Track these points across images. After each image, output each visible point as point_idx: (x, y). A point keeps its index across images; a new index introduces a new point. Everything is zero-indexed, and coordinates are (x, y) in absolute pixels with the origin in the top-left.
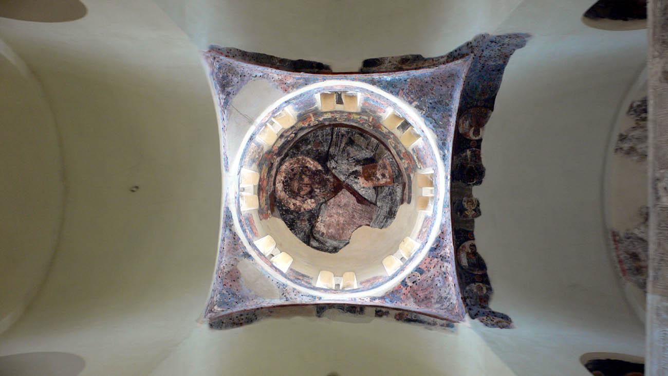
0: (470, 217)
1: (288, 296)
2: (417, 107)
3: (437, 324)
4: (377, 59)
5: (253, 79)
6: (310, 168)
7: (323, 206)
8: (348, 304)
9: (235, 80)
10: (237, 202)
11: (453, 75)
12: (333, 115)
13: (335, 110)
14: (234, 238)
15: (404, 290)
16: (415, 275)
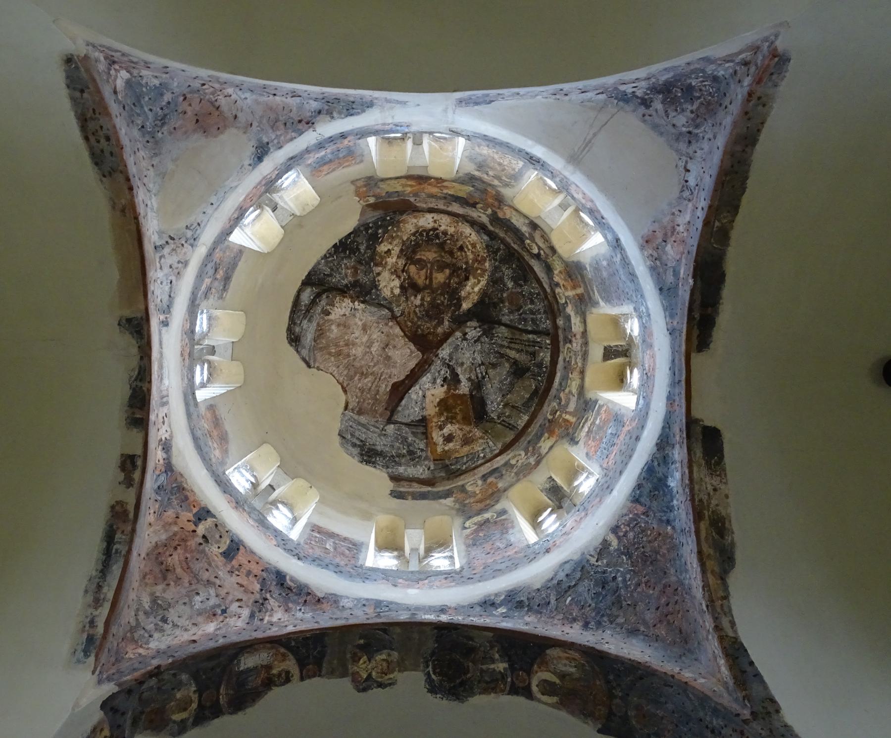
0: (352, 668)
2: (605, 544)
3: (96, 609)
7: (385, 312)
10: (387, 128)
11: (686, 643)
12: (578, 336)
13: (590, 340)
14: (300, 121)
15: (187, 515)
16: (223, 540)
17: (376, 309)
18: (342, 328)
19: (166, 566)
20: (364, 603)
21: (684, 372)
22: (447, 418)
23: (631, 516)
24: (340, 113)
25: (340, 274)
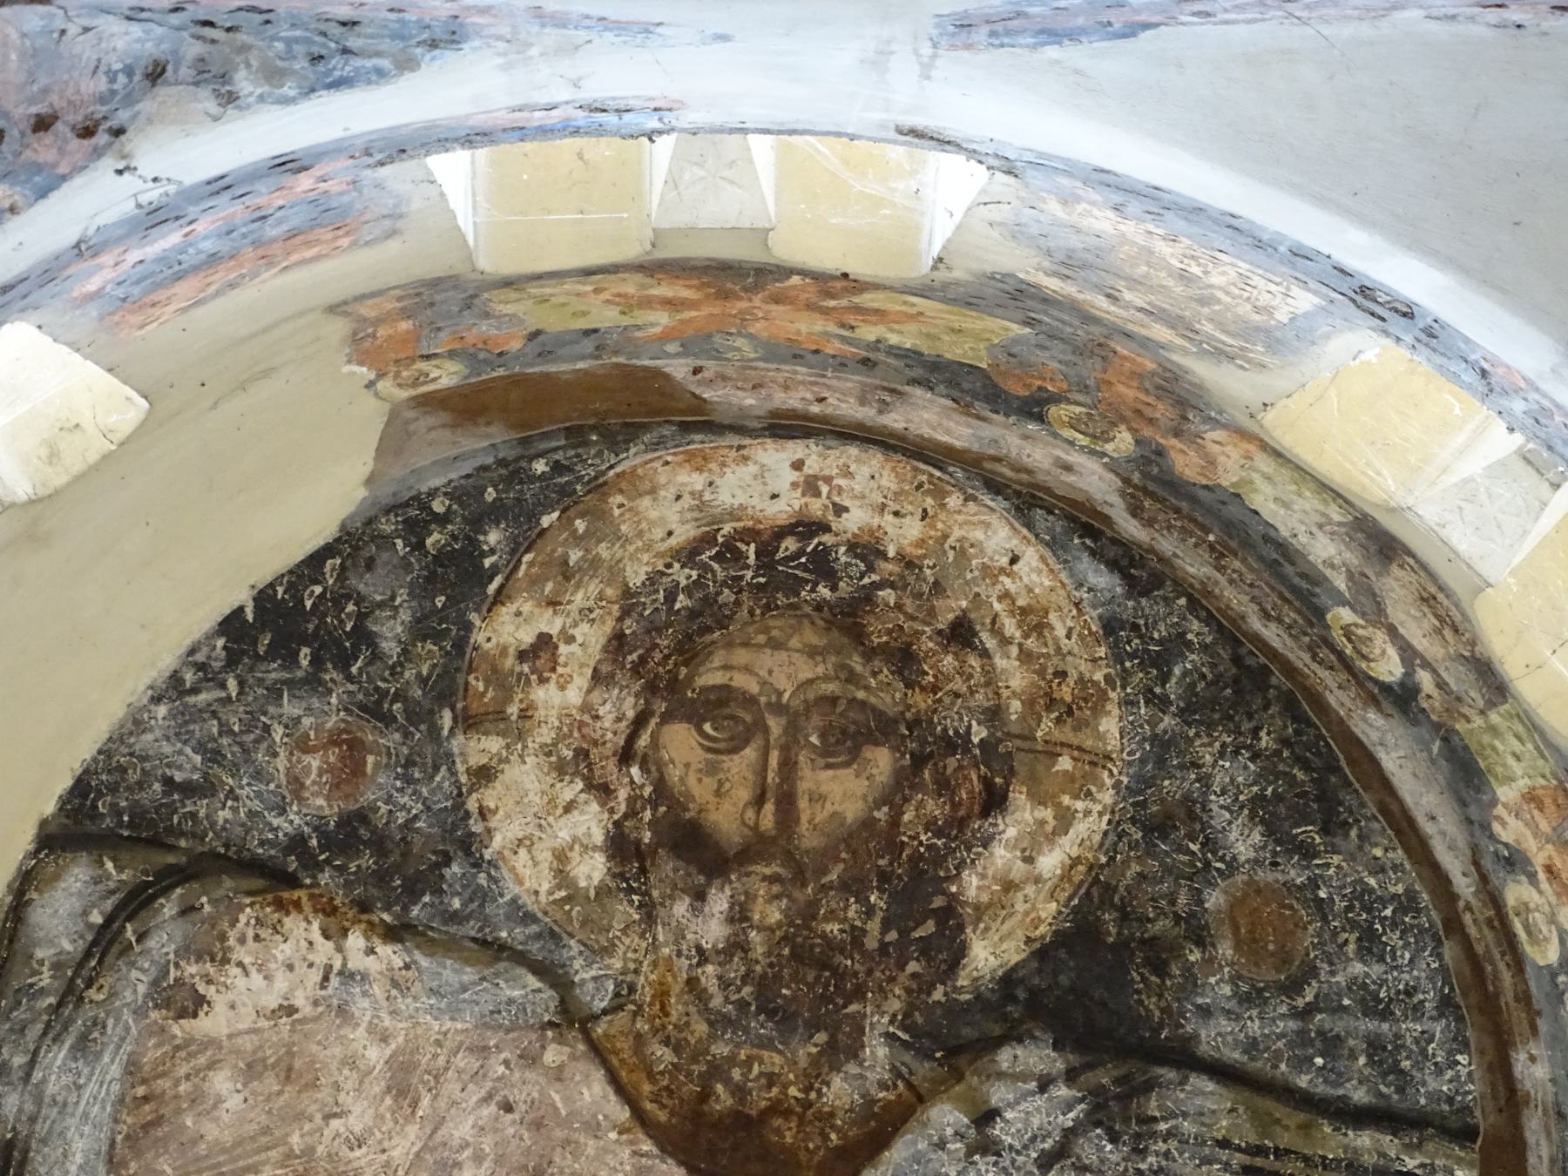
6: (986, 843)
7: (523, 987)
14: (43, 124)
17: (469, 974)
18: (271, 1083)
24: (273, 74)
25: (258, 775)
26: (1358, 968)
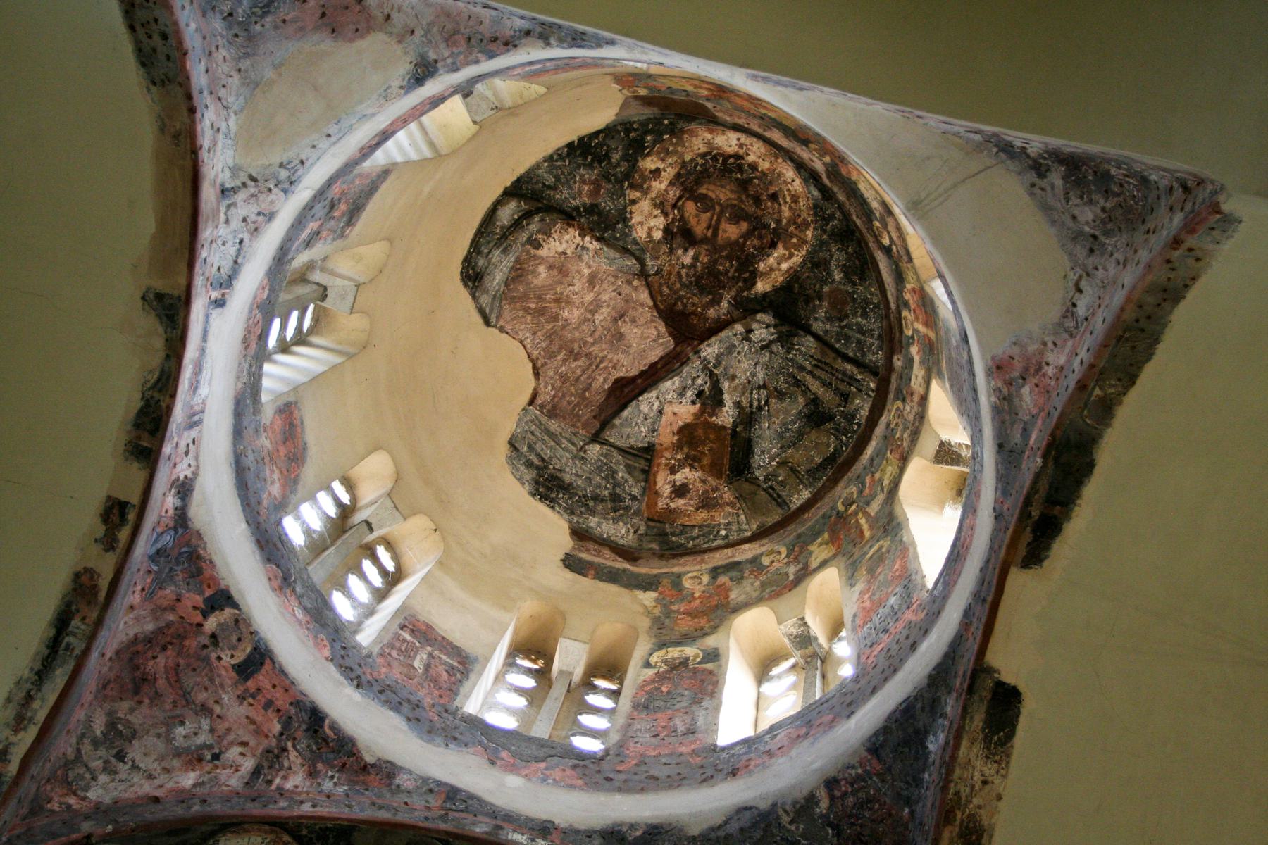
1: (241, 196)
2: (811, 799)
4: (1011, 735)
5: (1073, 277)
7: (631, 262)
8: (169, 409)
9: (1087, 214)
14: (495, 39)
16: (241, 646)
17: (617, 255)
18: (555, 272)
19: (144, 673)
20: (432, 787)
21: (993, 590)
22: (687, 457)
23: (860, 771)
25: (570, 188)
26: (859, 319)
